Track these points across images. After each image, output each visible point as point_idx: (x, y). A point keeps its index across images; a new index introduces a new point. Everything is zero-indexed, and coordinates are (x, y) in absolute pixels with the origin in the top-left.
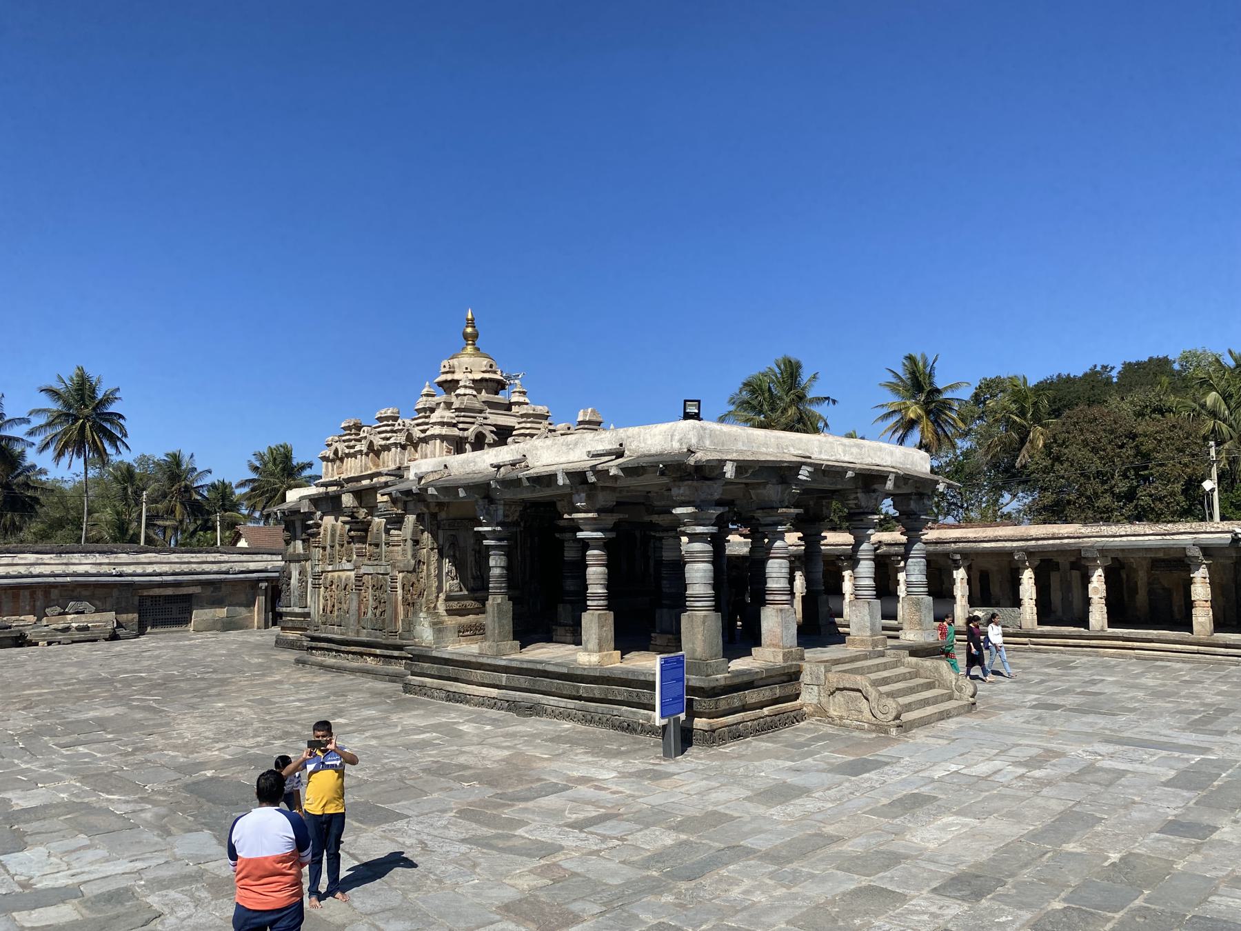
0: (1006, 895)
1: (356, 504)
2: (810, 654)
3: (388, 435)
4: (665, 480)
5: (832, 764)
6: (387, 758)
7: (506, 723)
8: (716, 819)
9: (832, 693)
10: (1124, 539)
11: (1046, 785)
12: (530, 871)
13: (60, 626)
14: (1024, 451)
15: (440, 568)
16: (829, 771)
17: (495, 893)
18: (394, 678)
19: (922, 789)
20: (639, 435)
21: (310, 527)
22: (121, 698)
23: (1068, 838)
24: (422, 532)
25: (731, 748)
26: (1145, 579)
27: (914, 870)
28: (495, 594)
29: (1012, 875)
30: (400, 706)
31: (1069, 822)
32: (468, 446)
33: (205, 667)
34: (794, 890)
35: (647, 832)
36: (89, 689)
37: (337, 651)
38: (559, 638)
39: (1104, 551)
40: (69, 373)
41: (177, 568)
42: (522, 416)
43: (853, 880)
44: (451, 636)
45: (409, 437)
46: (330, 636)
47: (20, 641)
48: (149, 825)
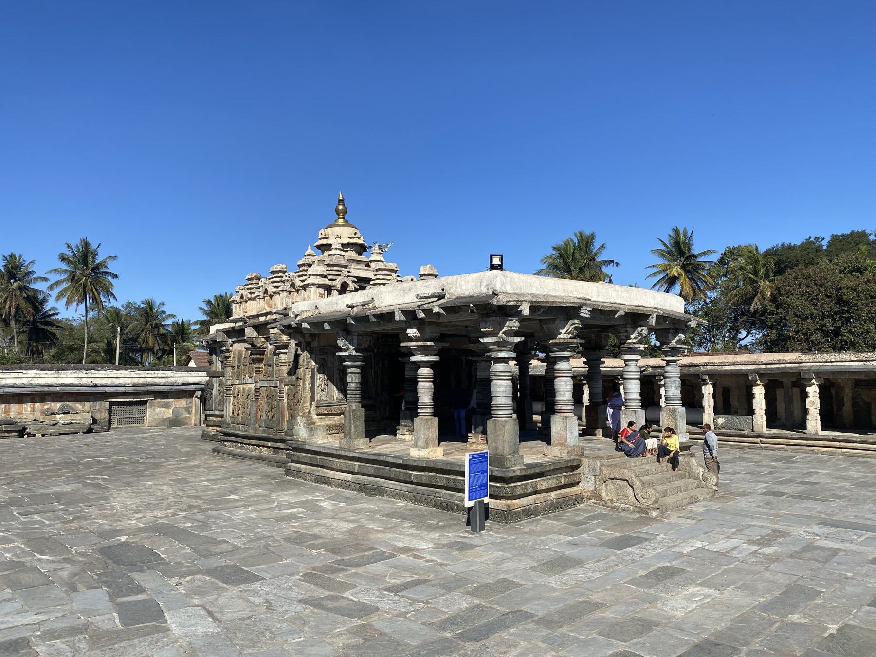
1: (255, 334)
3: (278, 284)
5: (604, 539)
6: (260, 528)
8: (505, 585)
10: (835, 364)
11: (774, 561)
14: (756, 299)
16: (601, 545)
18: (280, 464)
19: (673, 563)
20: (456, 281)
21: (222, 352)
23: (794, 608)
25: (526, 525)
26: (850, 394)
29: (747, 644)
30: (282, 485)
31: (794, 595)
34: (560, 654)
39: (818, 374)
40: (75, 243)
41: (136, 381)
42: (378, 270)
46: (236, 432)
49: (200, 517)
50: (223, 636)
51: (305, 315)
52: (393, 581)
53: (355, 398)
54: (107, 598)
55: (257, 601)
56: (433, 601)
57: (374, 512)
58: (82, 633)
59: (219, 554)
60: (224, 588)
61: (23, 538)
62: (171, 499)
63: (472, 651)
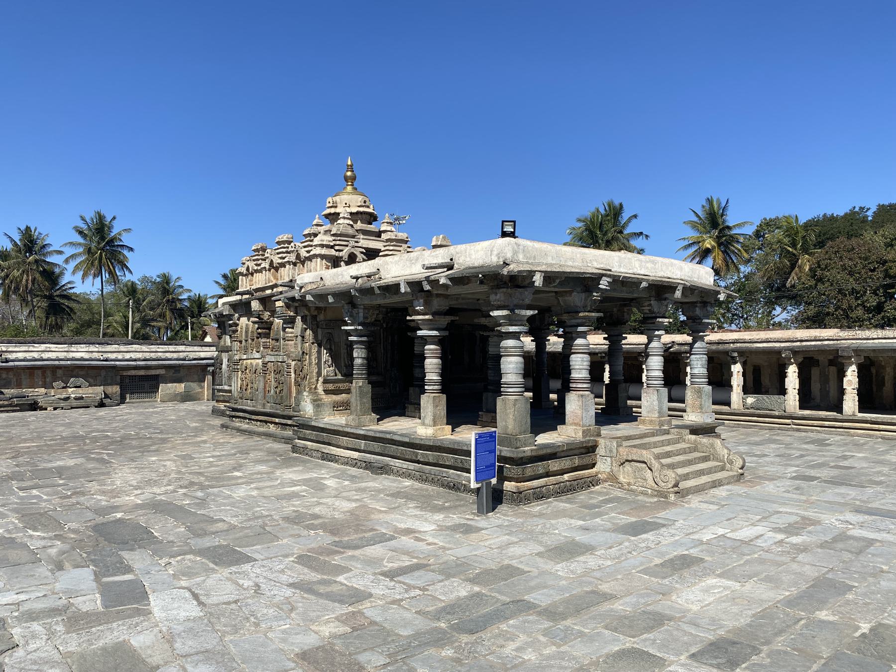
1: (261, 308)
2: (606, 430)
3: (284, 255)
4: (484, 288)
6: (259, 506)
7: (362, 479)
8: (509, 572)
9: (622, 464)
12: (337, 619)
13: (63, 397)
14: (793, 274)
15: (319, 358)
16: (614, 531)
17: (299, 639)
18: (287, 440)
19: (691, 551)
22: (84, 451)
24: (306, 329)
25: (536, 507)
28: (357, 378)
30: (287, 462)
32: (342, 263)
33: (155, 429)
34: (563, 649)
35: (447, 583)
36: (67, 443)
37: (250, 419)
38: (409, 414)
39: (857, 351)
40: (90, 215)
41: (147, 355)
42: (387, 240)
45: (298, 256)
46: (244, 408)
47: (34, 406)
48: (50, 560)
49: (200, 494)
50: (206, 621)
52: (391, 565)
53: (362, 374)
54: (92, 577)
55: (246, 583)
56: (430, 588)
57: (379, 491)
58: (60, 615)
59: (214, 533)
60: (213, 569)
61: (17, 513)
62: (173, 475)
63: (466, 644)
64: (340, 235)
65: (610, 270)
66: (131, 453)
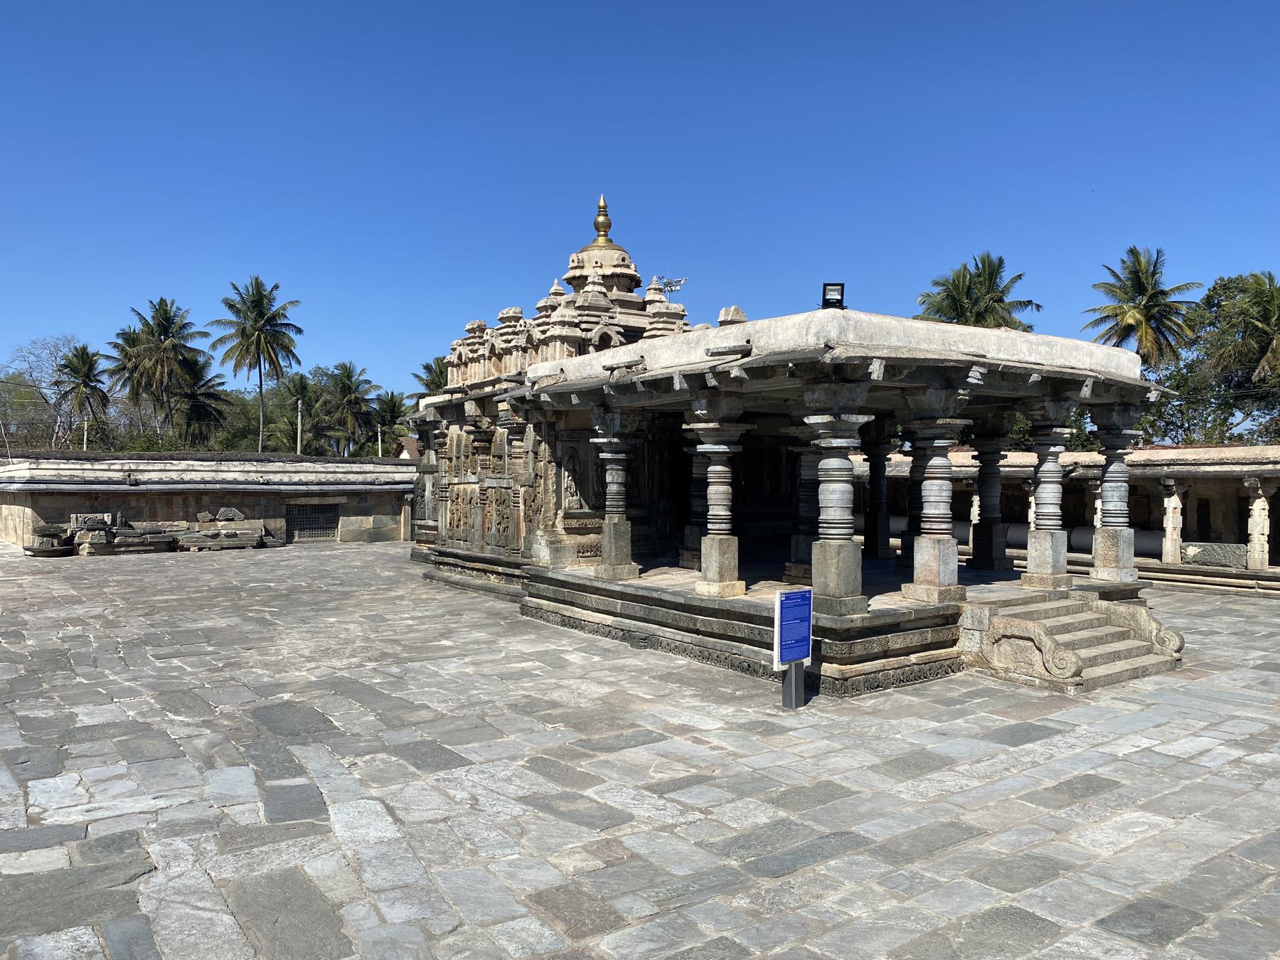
0: (1204, 940)
1: (479, 412)
2: (972, 592)
3: (510, 337)
4: (797, 383)
5: (988, 728)
8: (828, 792)
9: (997, 641)
11: (1270, 776)
12: (584, 848)
13: (210, 533)
14: (1263, 362)
15: (558, 482)
16: (985, 737)
17: (532, 874)
18: (514, 597)
19: (1100, 770)
20: (769, 328)
24: (540, 442)
25: (869, 701)
27: (1075, 888)
28: (612, 512)
29: (1216, 907)
30: (514, 628)
32: (591, 349)
33: (334, 578)
34: (907, 904)
35: (739, 804)
37: (463, 567)
38: (685, 564)
40: (244, 282)
41: (323, 477)
42: (655, 315)
43: (990, 895)
44: (570, 557)
45: (529, 339)
46: (456, 551)
49: (395, 670)
50: (405, 845)
51: (545, 383)
52: (659, 775)
55: (460, 795)
56: (715, 810)
57: (642, 671)
59: (415, 724)
60: (414, 774)
62: (359, 643)
63: (767, 891)
64: (588, 308)
65: (984, 357)
66: (302, 611)
